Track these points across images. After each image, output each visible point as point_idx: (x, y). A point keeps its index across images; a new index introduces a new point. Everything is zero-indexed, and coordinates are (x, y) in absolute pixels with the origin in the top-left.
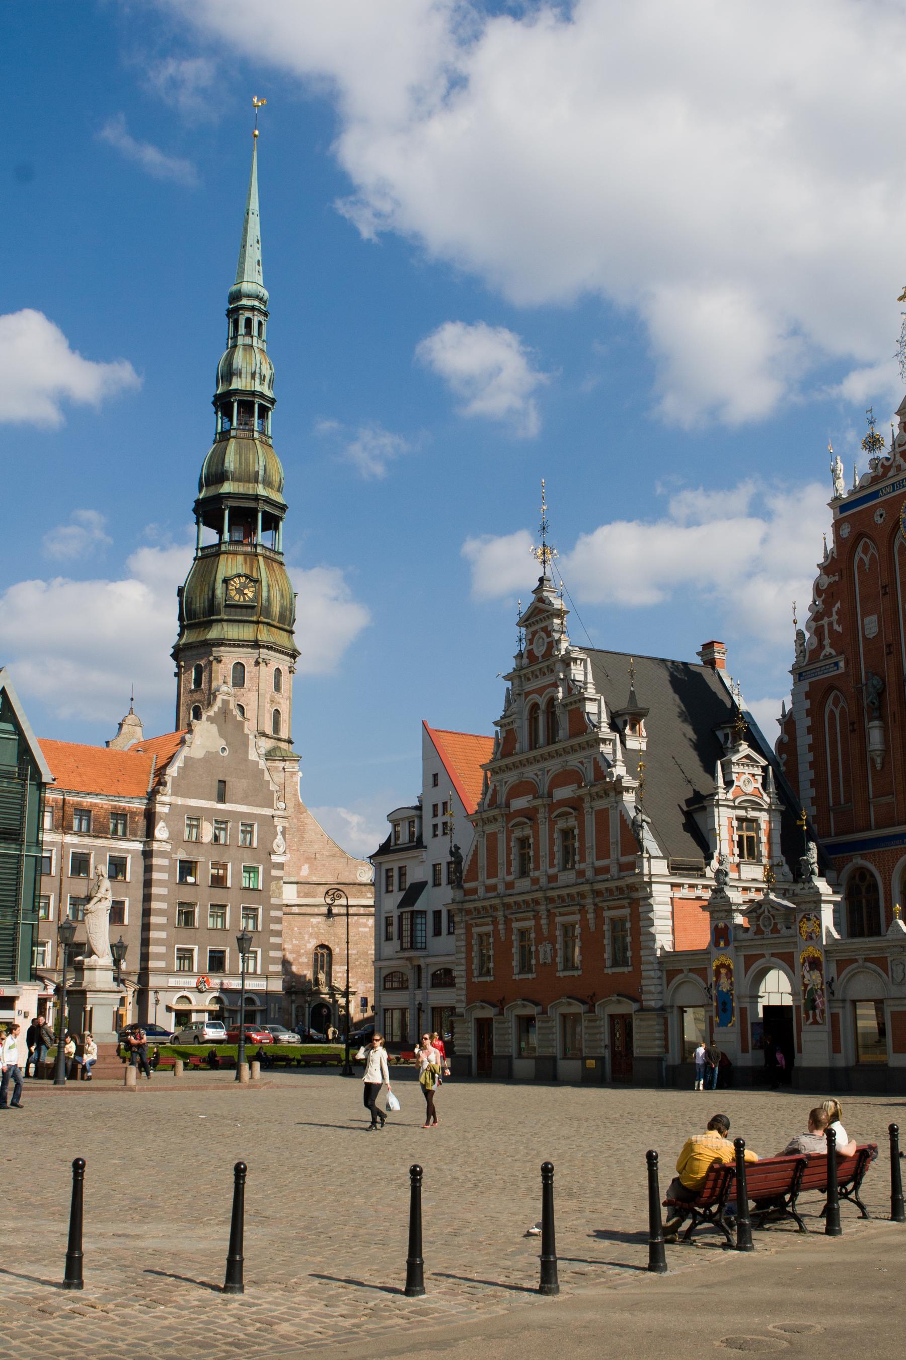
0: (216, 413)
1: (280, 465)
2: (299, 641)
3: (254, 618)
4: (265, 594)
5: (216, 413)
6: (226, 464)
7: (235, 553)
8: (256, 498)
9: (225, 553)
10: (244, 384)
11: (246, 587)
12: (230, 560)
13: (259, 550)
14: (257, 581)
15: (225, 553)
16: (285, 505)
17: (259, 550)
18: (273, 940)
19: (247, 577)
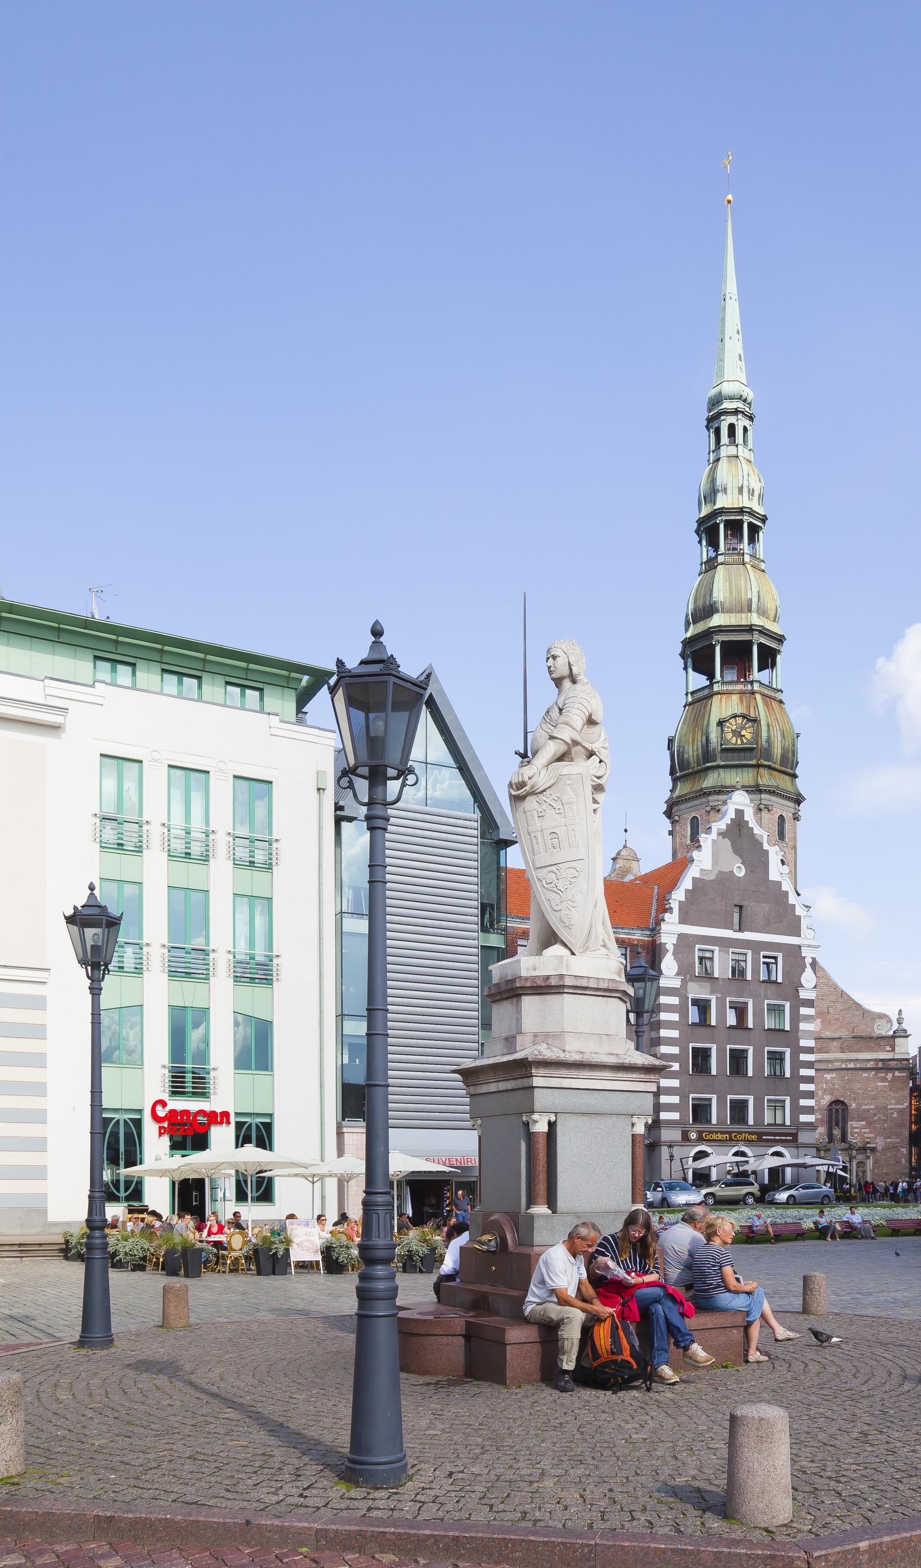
0: (700, 542)
1: (775, 592)
3: (753, 762)
4: (764, 734)
5: (700, 542)
6: (715, 594)
7: (730, 693)
8: (750, 629)
9: (718, 693)
10: (730, 501)
11: (743, 728)
12: (724, 700)
13: (756, 687)
14: (755, 721)
15: (718, 693)
16: (782, 636)
17: (756, 687)
19: (744, 717)
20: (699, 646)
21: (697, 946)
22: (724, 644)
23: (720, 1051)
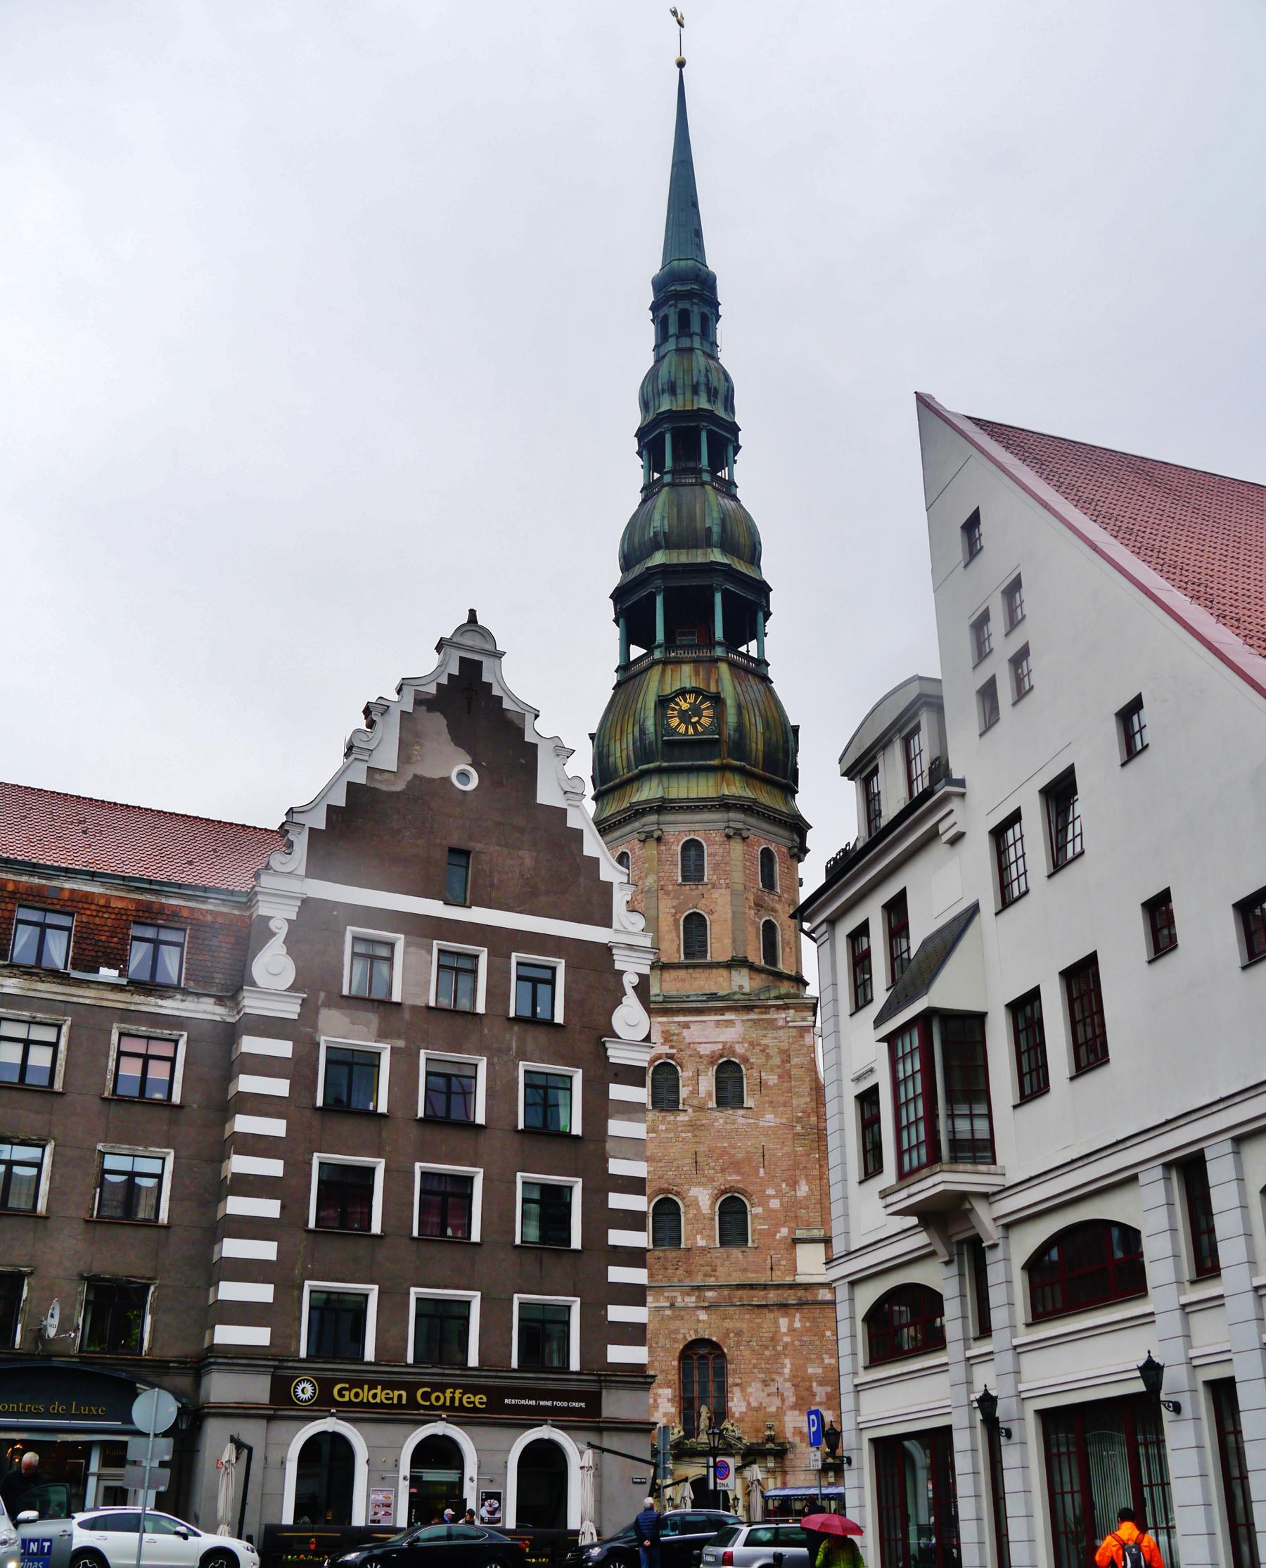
3: (715, 762)
4: (731, 717)
7: (679, 662)
14: (717, 700)
18: (618, 1274)
21: (350, 931)
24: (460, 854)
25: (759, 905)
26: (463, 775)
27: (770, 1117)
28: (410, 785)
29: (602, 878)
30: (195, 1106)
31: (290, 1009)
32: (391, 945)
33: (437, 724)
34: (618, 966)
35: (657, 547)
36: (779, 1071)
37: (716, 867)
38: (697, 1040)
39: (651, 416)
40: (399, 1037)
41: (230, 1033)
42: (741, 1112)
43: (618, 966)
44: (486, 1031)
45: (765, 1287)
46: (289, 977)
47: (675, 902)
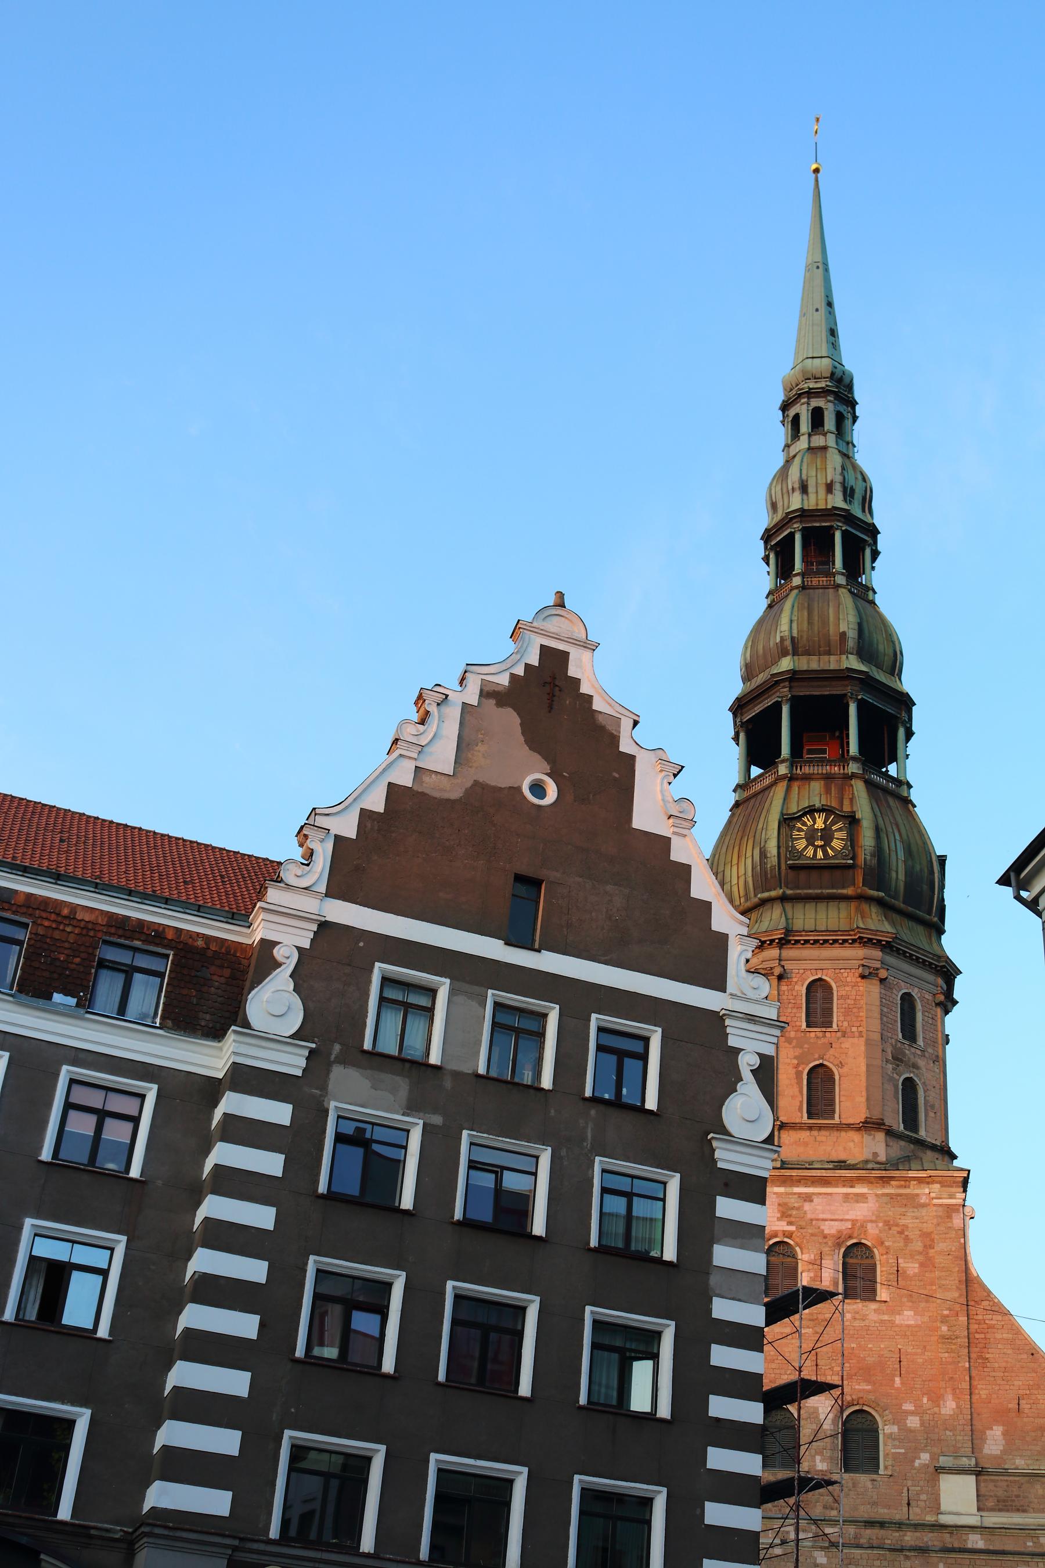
2: (953, 944)
3: (849, 891)
4: (867, 839)
7: (807, 778)
14: (852, 821)
18: (721, 1459)
20: (758, 709)
21: (379, 969)
22: (796, 703)
23: (422, 1302)
24: (529, 883)
25: (898, 1059)
26: (538, 789)
27: (909, 1313)
28: (469, 792)
29: (714, 928)
30: (159, 1183)
31: (292, 1062)
32: (432, 992)
33: (510, 719)
34: (732, 1042)
35: (784, 653)
36: (921, 1258)
37: (847, 1012)
38: (821, 1216)
39: (780, 515)
40: (435, 1110)
41: (210, 1090)
42: (873, 1306)
43: (732, 1042)
44: (552, 1113)
45: (900, 1525)
46: (295, 1021)
47: (798, 1052)
